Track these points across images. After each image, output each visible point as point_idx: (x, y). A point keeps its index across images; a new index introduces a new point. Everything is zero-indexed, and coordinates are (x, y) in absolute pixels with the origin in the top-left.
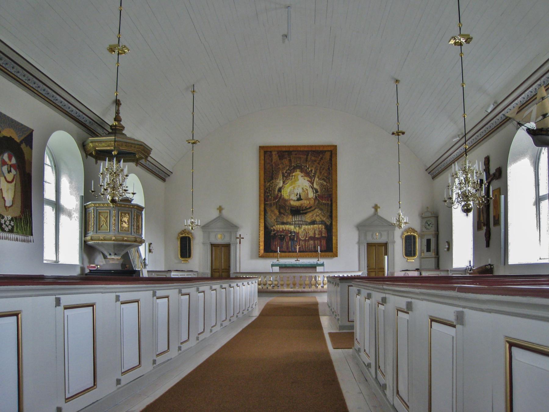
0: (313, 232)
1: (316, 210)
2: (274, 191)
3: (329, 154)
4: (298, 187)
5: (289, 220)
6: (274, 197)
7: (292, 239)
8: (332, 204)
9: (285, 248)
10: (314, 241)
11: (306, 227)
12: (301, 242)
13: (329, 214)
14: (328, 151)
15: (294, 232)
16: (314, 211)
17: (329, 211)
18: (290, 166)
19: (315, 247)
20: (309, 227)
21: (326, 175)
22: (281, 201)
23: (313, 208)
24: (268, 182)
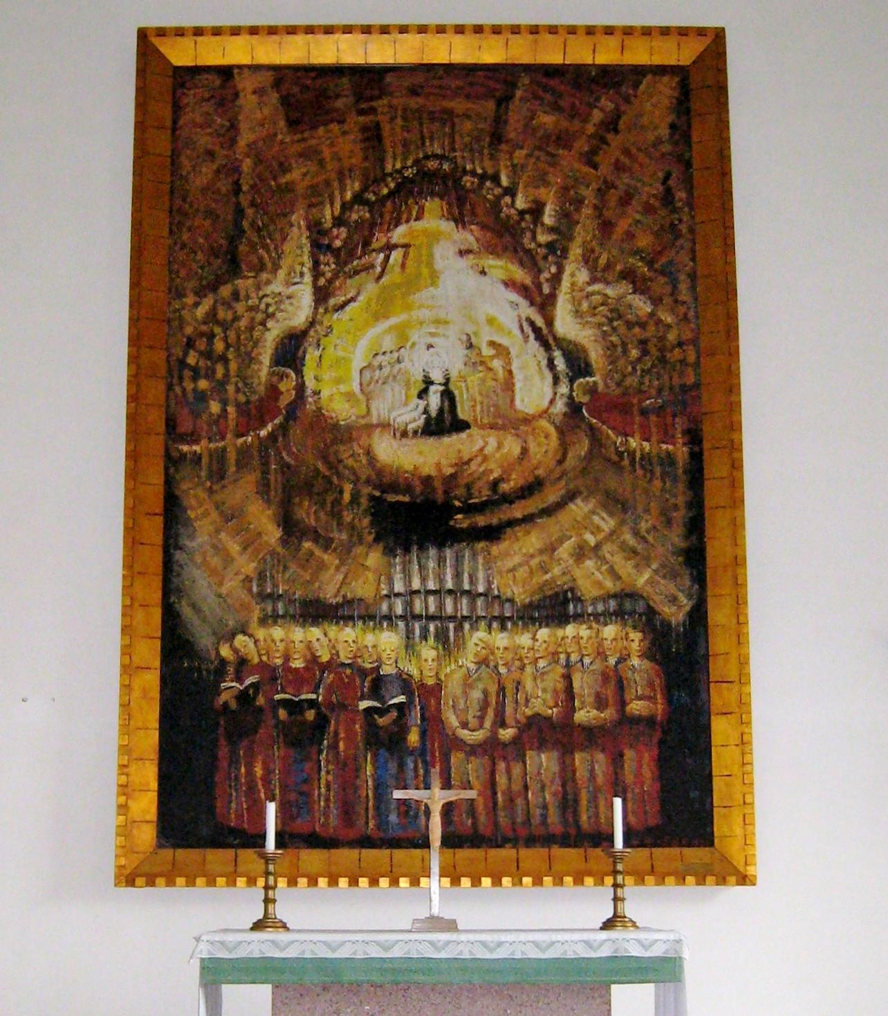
0: (554, 679)
1: (579, 508)
2: (249, 359)
3: (666, 89)
4: (431, 336)
5: (363, 588)
6: (243, 409)
7: (386, 741)
8: (697, 458)
9: (326, 816)
10: (567, 751)
11: (501, 640)
12: (456, 758)
13: (676, 537)
14: (661, 70)
15: (405, 683)
16: (564, 517)
17: (680, 515)
18: (373, 179)
19: (568, 803)
20: (524, 640)
21: (644, 241)
22: (296, 432)
23: (552, 496)
24: (200, 293)
